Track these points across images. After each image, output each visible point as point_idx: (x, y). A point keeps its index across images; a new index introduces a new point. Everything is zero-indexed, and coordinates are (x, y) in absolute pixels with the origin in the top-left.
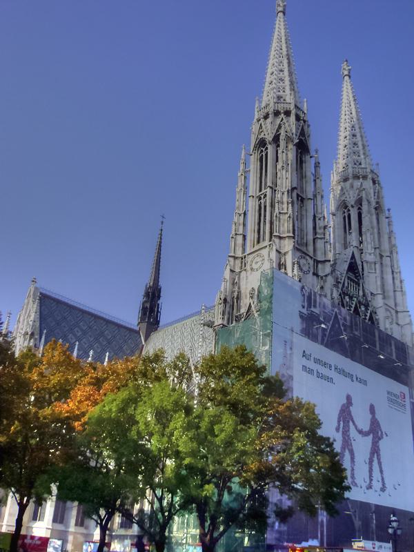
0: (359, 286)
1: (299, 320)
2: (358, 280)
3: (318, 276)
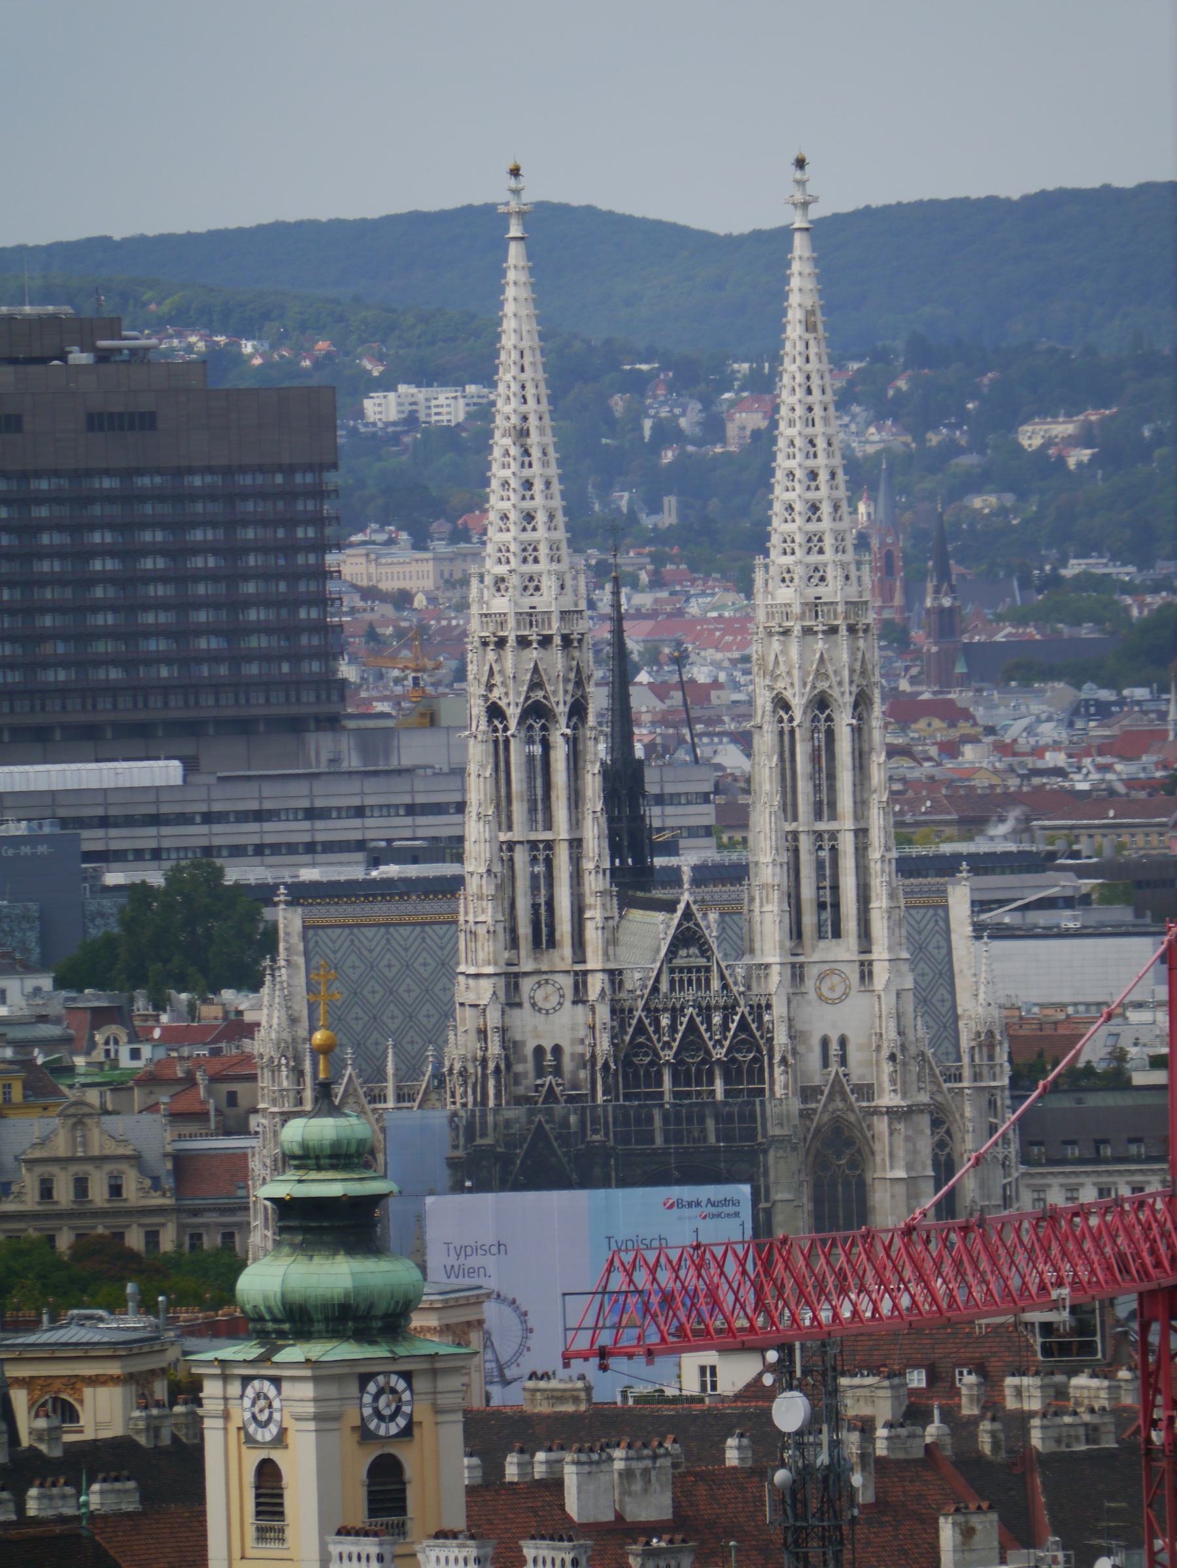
0: (708, 969)
1: (447, 1172)
2: (708, 959)
3: (584, 1002)
